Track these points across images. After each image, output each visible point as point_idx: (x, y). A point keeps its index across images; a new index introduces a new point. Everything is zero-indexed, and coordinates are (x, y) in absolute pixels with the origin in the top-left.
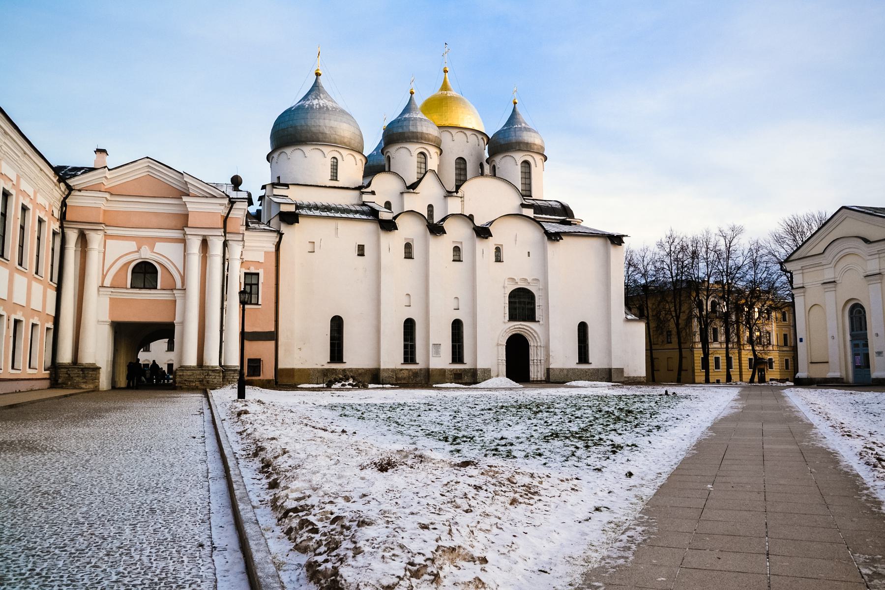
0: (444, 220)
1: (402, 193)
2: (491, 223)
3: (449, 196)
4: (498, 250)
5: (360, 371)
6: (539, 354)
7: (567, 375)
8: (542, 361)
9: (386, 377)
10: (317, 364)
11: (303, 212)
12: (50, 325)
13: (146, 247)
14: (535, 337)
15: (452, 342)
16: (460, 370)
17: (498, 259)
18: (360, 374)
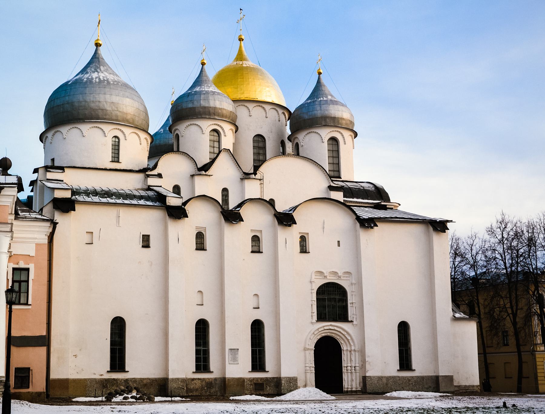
0: (240, 205)
1: (192, 176)
2: (295, 208)
3: (246, 178)
4: (303, 239)
5: (145, 382)
6: (353, 359)
7: (387, 384)
8: (357, 368)
9: (175, 388)
10: (95, 374)
11: (80, 198)
14: (348, 340)
15: (252, 347)
16: (261, 379)
17: (304, 250)
18: (145, 385)
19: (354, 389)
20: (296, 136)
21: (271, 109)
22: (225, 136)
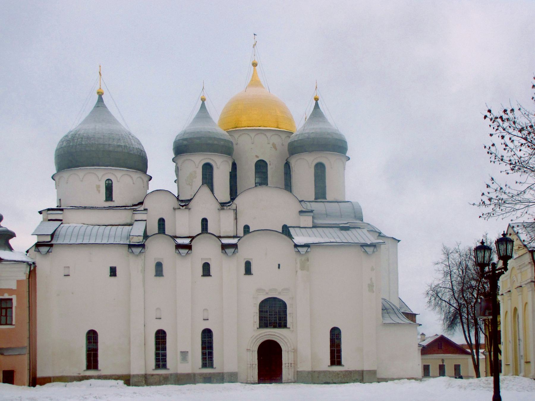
3: (222, 209)
14: (286, 343)
16: (210, 374)
21: (271, 136)
22: (217, 168)
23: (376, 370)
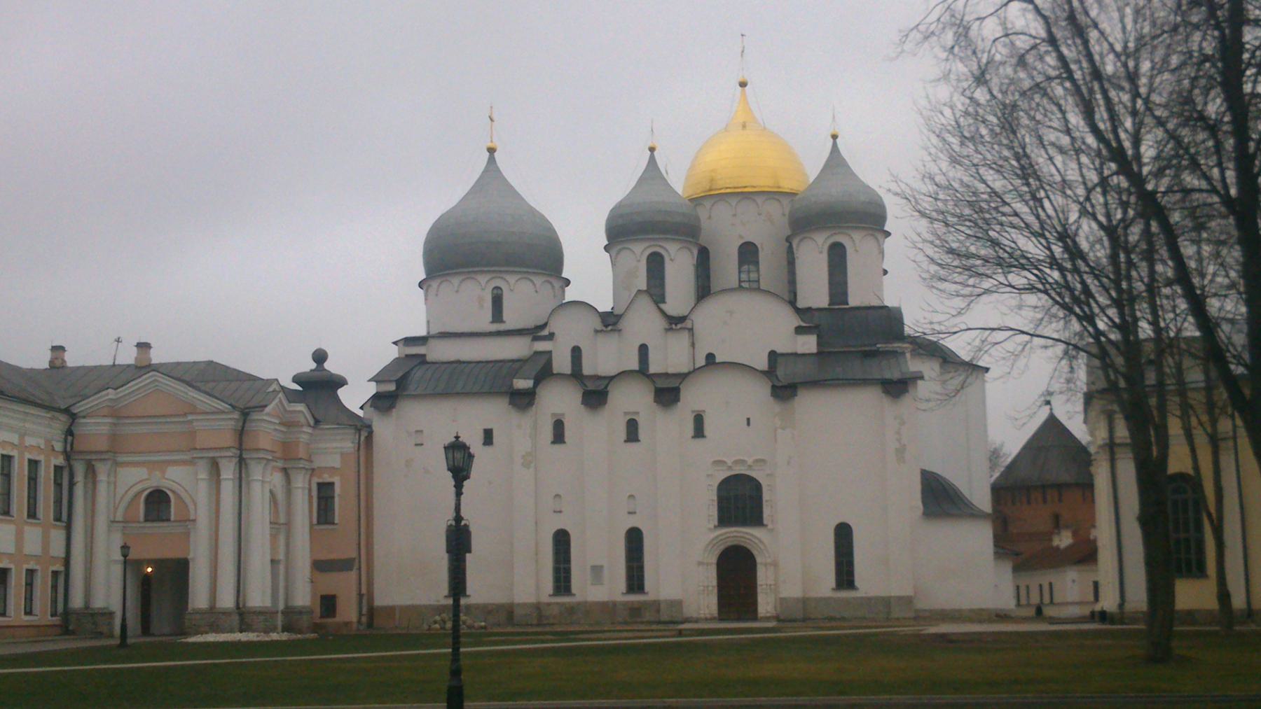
1: (597, 331)
4: (699, 421)
12: (59, 567)
13: (157, 473)
16: (639, 602)
17: (699, 432)
19: (768, 615)
20: (813, 236)
23: (911, 597)
